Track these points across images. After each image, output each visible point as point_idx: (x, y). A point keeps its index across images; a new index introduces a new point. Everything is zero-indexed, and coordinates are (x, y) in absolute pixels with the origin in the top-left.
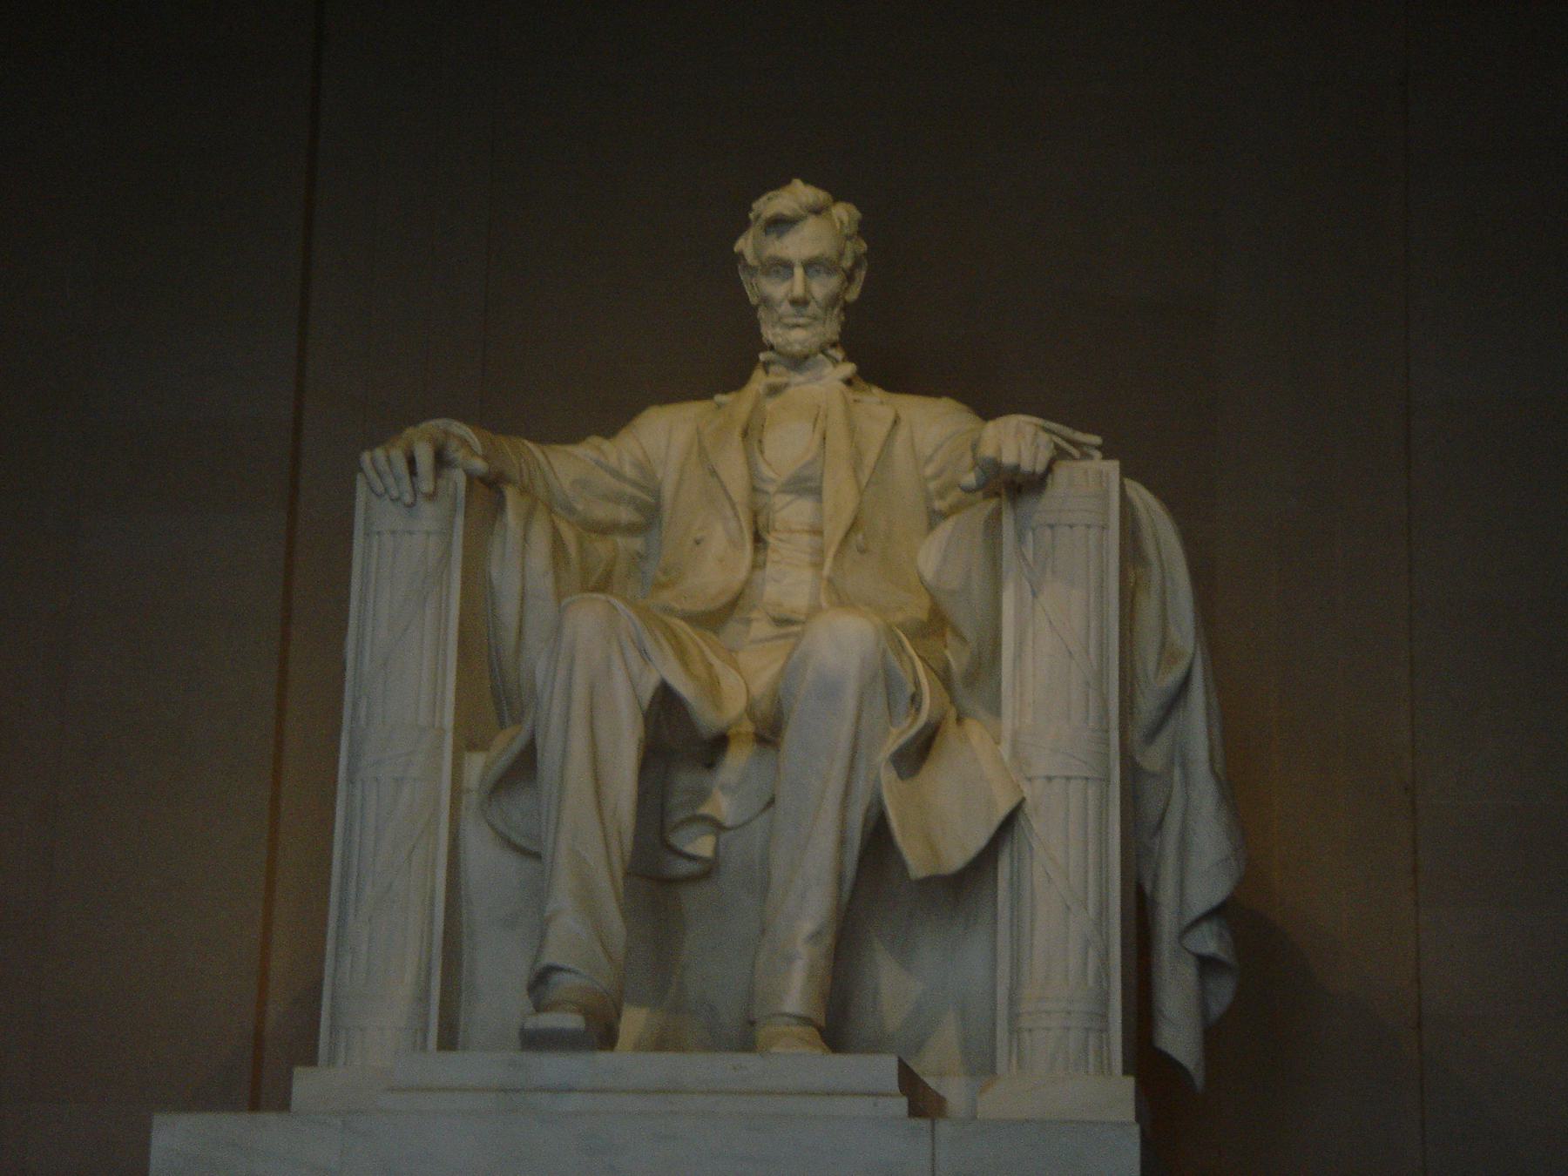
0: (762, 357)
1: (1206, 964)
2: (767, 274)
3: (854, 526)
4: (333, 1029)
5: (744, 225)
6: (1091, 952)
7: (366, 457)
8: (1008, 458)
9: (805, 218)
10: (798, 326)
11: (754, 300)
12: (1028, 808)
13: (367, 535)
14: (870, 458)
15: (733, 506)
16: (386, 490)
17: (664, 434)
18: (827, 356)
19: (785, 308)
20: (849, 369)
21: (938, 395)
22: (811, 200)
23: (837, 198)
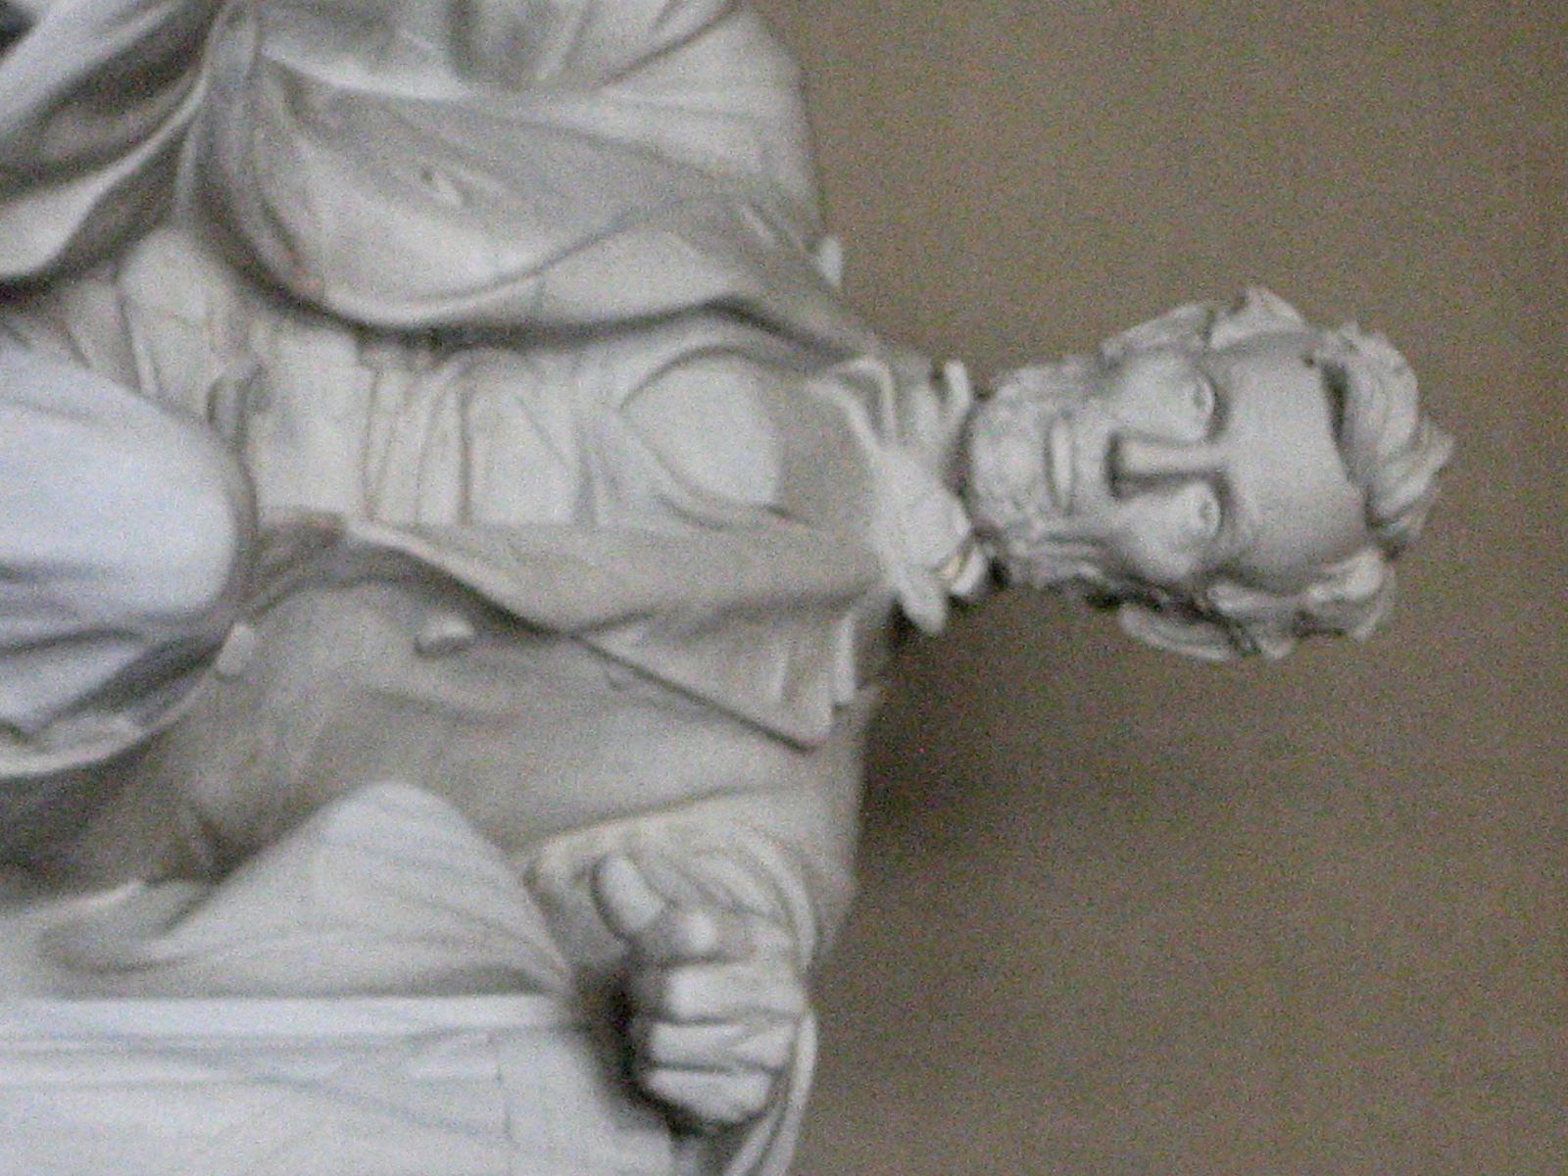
0: (957, 374)
8: (688, 990)
9: (1351, 475)
14: (681, 668)
15: (536, 271)
18: (965, 553)
20: (927, 610)
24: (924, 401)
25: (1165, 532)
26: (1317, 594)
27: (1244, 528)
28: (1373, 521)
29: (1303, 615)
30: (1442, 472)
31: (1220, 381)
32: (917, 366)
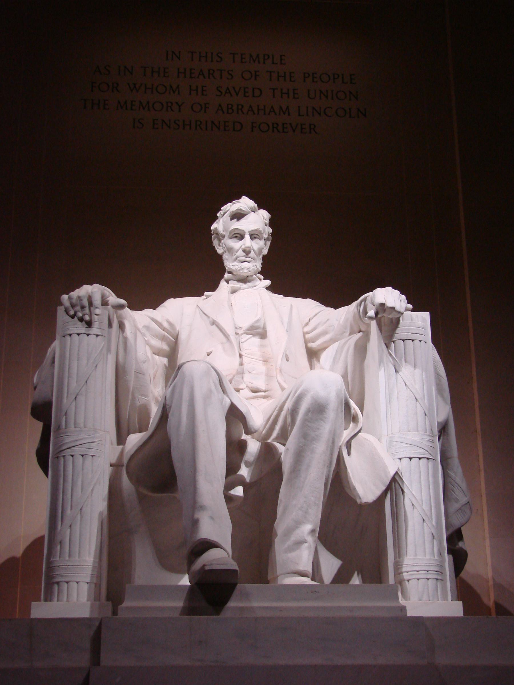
0: (226, 276)
2: (231, 238)
5: (215, 218)
6: (435, 541)
9: (250, 213)
11: (220, 251)
14: (286, 319)
17: (178, 311)
19: (240, 253)
20: (268, 283)
21: (305, 298)
22: (253, 206)
23: (260, 207)
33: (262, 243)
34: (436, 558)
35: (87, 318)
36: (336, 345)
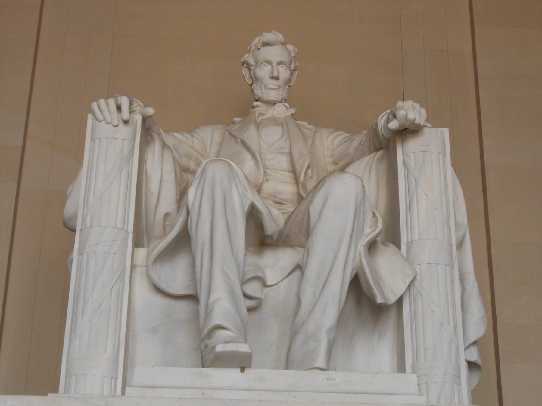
0: (255, 104)
1: (472, 365)
3: (308, 167)
4: (66, 377)
7: (94, 105)
8: (411, 116)
10: (273, 89)
12: (418, 277)
13: (93, 140)
14: (310, 142)
16: (105, 119)
20: (293, 111)
24: (258, 109)
25: (284, 73)
26: (293, 54)
27: (287, 60)
28: (283, 44)
29: (294, 57)
30: (279, 32)
31: (262, 62)
32: (252, 110)
33: (289, 73)
34: (453, 360)
35: (116, 124)
36: (357, 163)
